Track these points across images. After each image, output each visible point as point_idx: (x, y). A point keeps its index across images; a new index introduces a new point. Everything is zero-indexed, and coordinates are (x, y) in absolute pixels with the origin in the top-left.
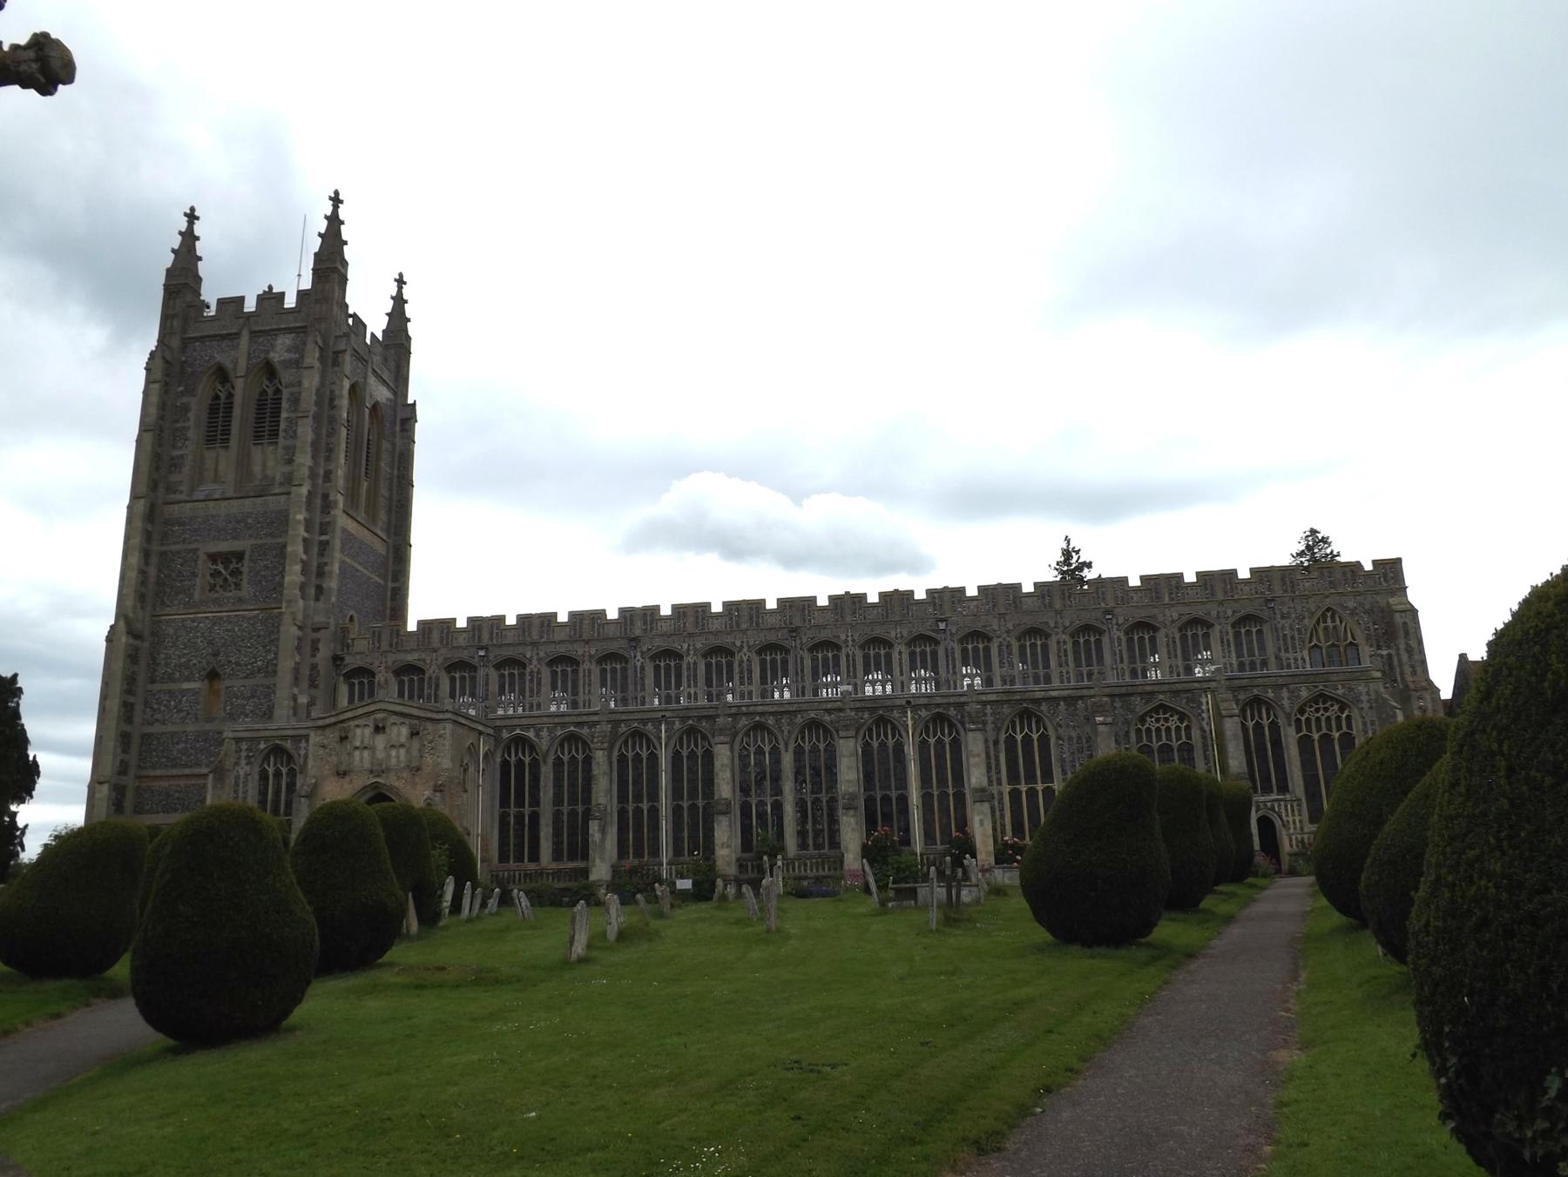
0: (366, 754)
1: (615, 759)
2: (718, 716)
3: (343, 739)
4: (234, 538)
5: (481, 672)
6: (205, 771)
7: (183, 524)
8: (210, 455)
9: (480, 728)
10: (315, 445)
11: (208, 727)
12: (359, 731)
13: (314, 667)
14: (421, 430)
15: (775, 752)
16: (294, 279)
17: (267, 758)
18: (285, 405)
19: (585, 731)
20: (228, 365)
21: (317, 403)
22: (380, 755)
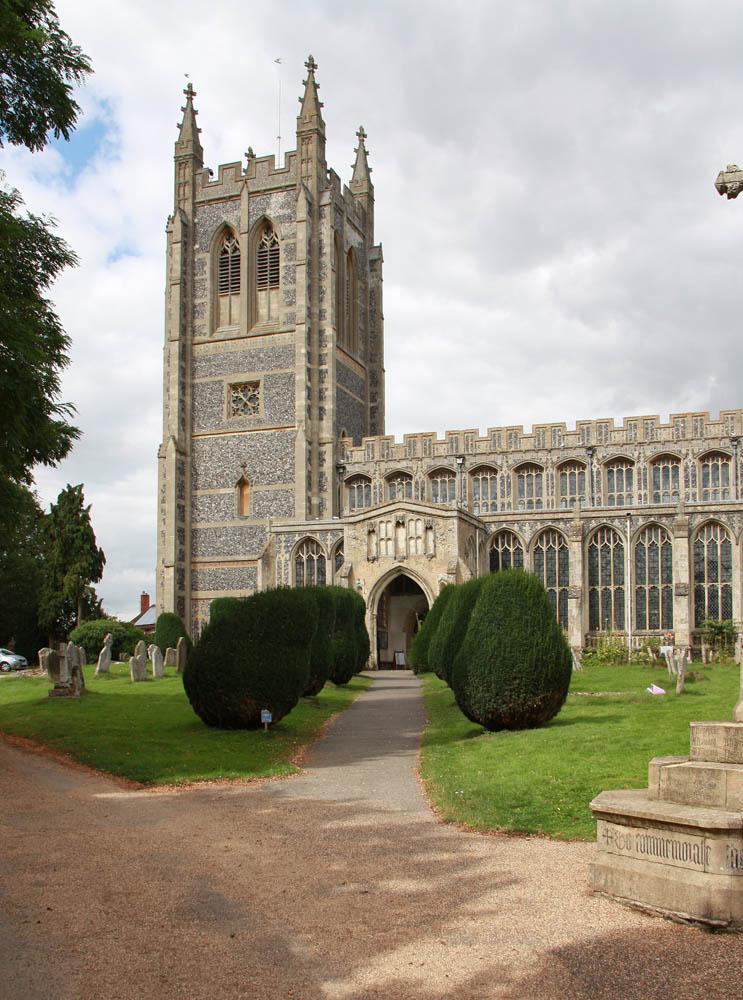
0: (390, 543)
1: (586, 550)
2: (677, 514)
3: (371, 532)
4: (250, 370)
5: (458, 478)
6: (255, 557)
7: (209, 360)
8: (224, 301)
9: (476, 523)
11: (242, 523)
12: (383, 526)
13: (321, 475)
14: (387, 269)
15: (726, 545)
17: (300, 547)
18: (282, 255)
19: (561, 525)
20: (233, 223)
21: (309, 252)
22: (402, 545)
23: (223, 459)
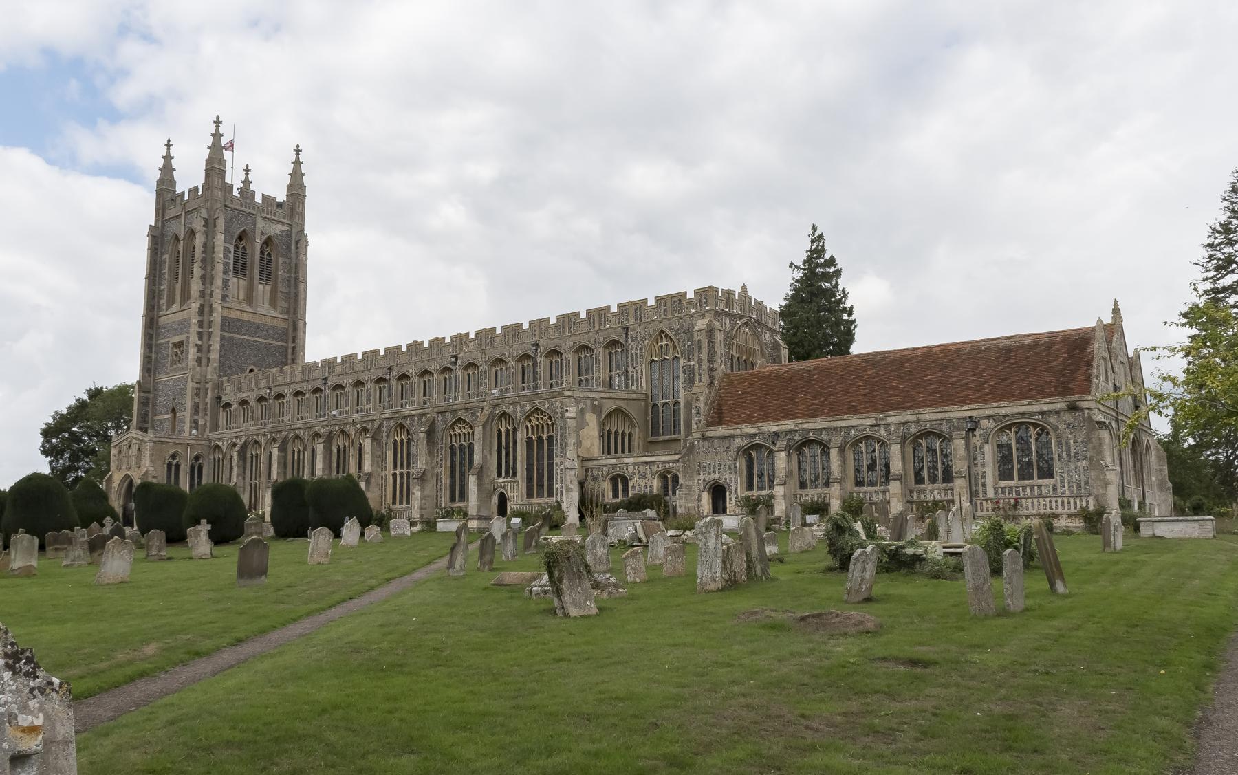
10: (203, 277)
16: (199, 180)
23: (167, 395)
